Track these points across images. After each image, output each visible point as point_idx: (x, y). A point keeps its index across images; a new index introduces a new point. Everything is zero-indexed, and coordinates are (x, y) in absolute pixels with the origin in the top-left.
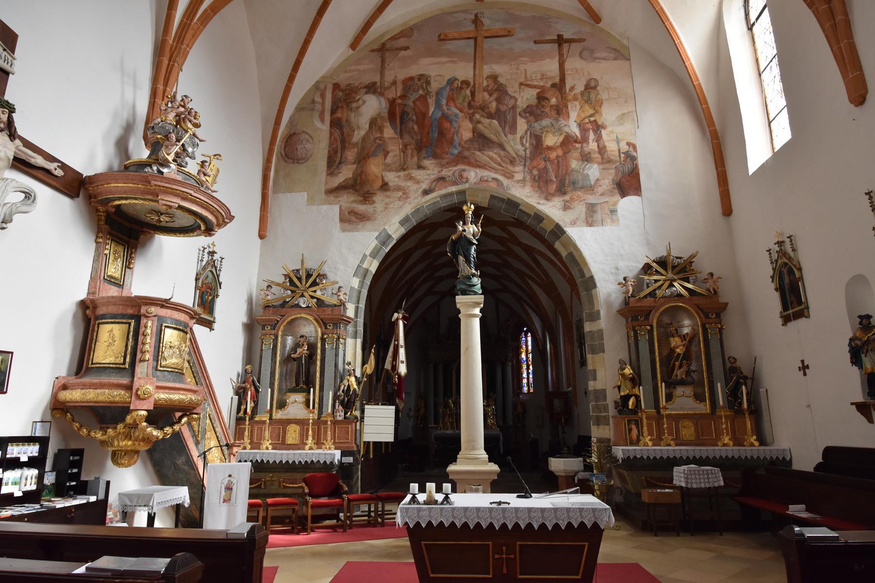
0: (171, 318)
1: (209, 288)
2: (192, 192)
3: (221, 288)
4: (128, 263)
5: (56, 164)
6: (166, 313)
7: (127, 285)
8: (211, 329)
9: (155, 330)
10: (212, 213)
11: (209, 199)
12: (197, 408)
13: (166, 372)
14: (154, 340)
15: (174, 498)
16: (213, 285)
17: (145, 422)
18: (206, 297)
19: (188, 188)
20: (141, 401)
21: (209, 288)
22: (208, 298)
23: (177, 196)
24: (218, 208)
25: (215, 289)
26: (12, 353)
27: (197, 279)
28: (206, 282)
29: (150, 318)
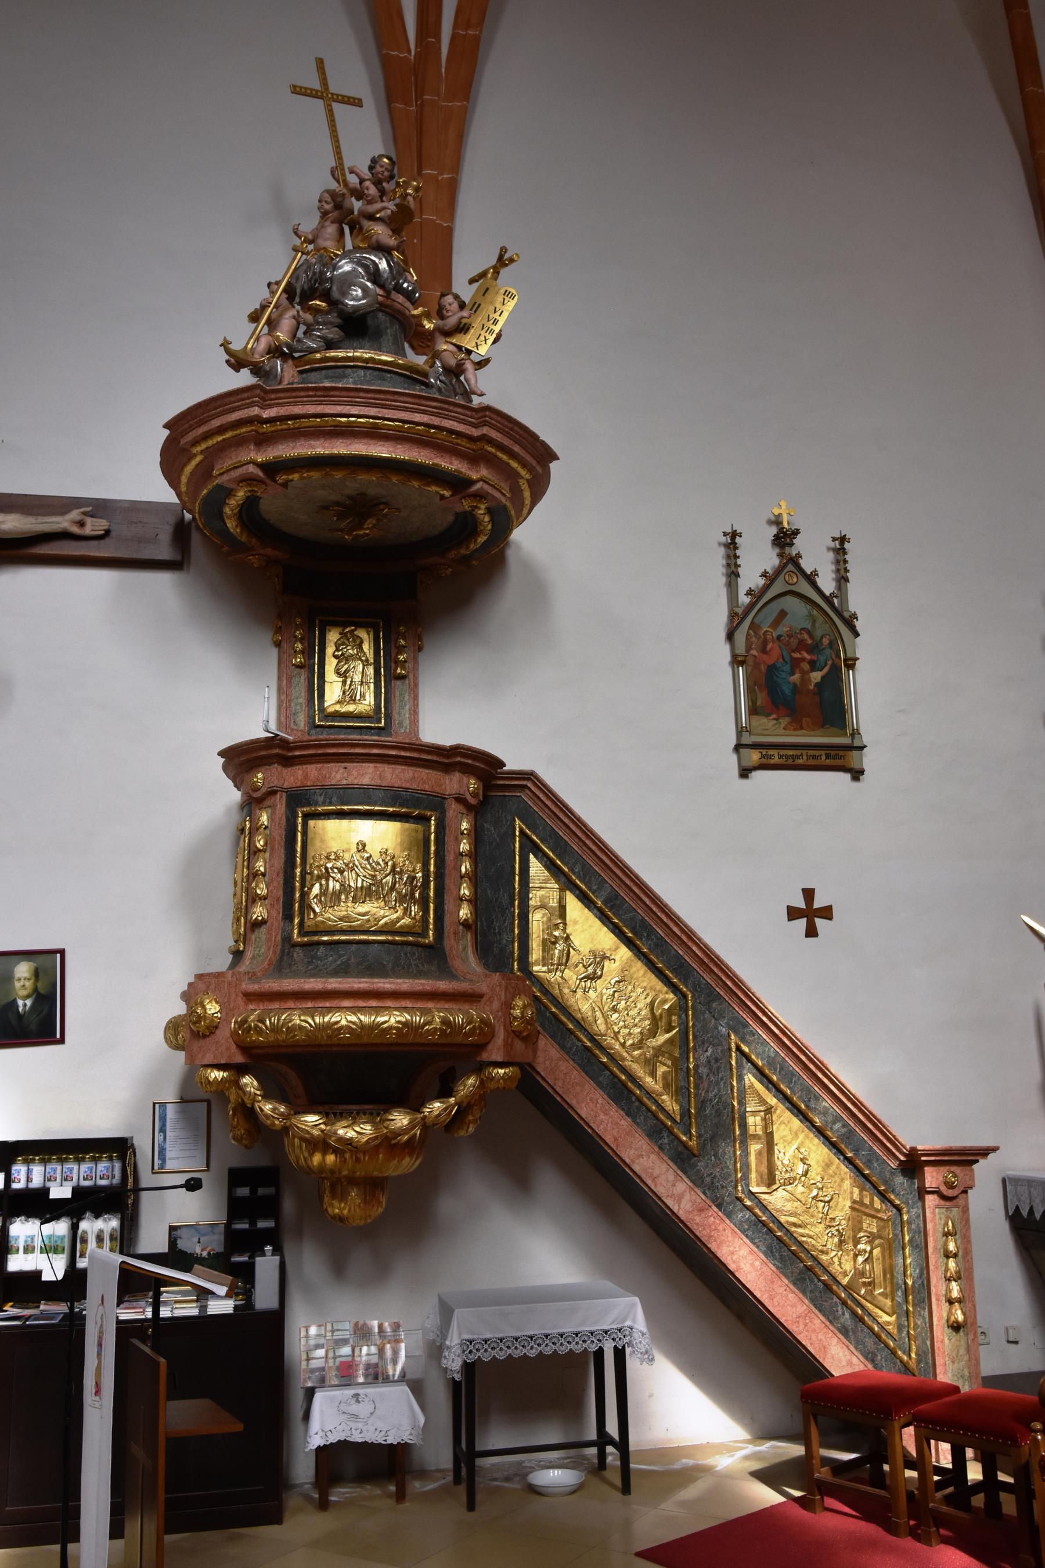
0: (323, 788)
1: (802, 646)
2: (255, 411)
3: (856, 634)
4: (393, 665)
5: (75, 515)
6: (306, 777)
7: (401, 724)
8: (857, 774)
9: (279, 834)
10: (373, 433)
11: (321, 403)
12: (490, 1047)
13: (322, 948)
14: (279, 861)
15: (566, 1329)
16: (818, 633)
17: (267, 1097)
18: (796, 678)
19: (239, 408)
20: (202, 1042)
21: (802, 646)
22: (805, 679)
23: (240, 442)
24: (373, 411)
25: (832, 645)
26: (62, 952)
27: (730, 637)
28: (782, 630)
29: (267, 803)
